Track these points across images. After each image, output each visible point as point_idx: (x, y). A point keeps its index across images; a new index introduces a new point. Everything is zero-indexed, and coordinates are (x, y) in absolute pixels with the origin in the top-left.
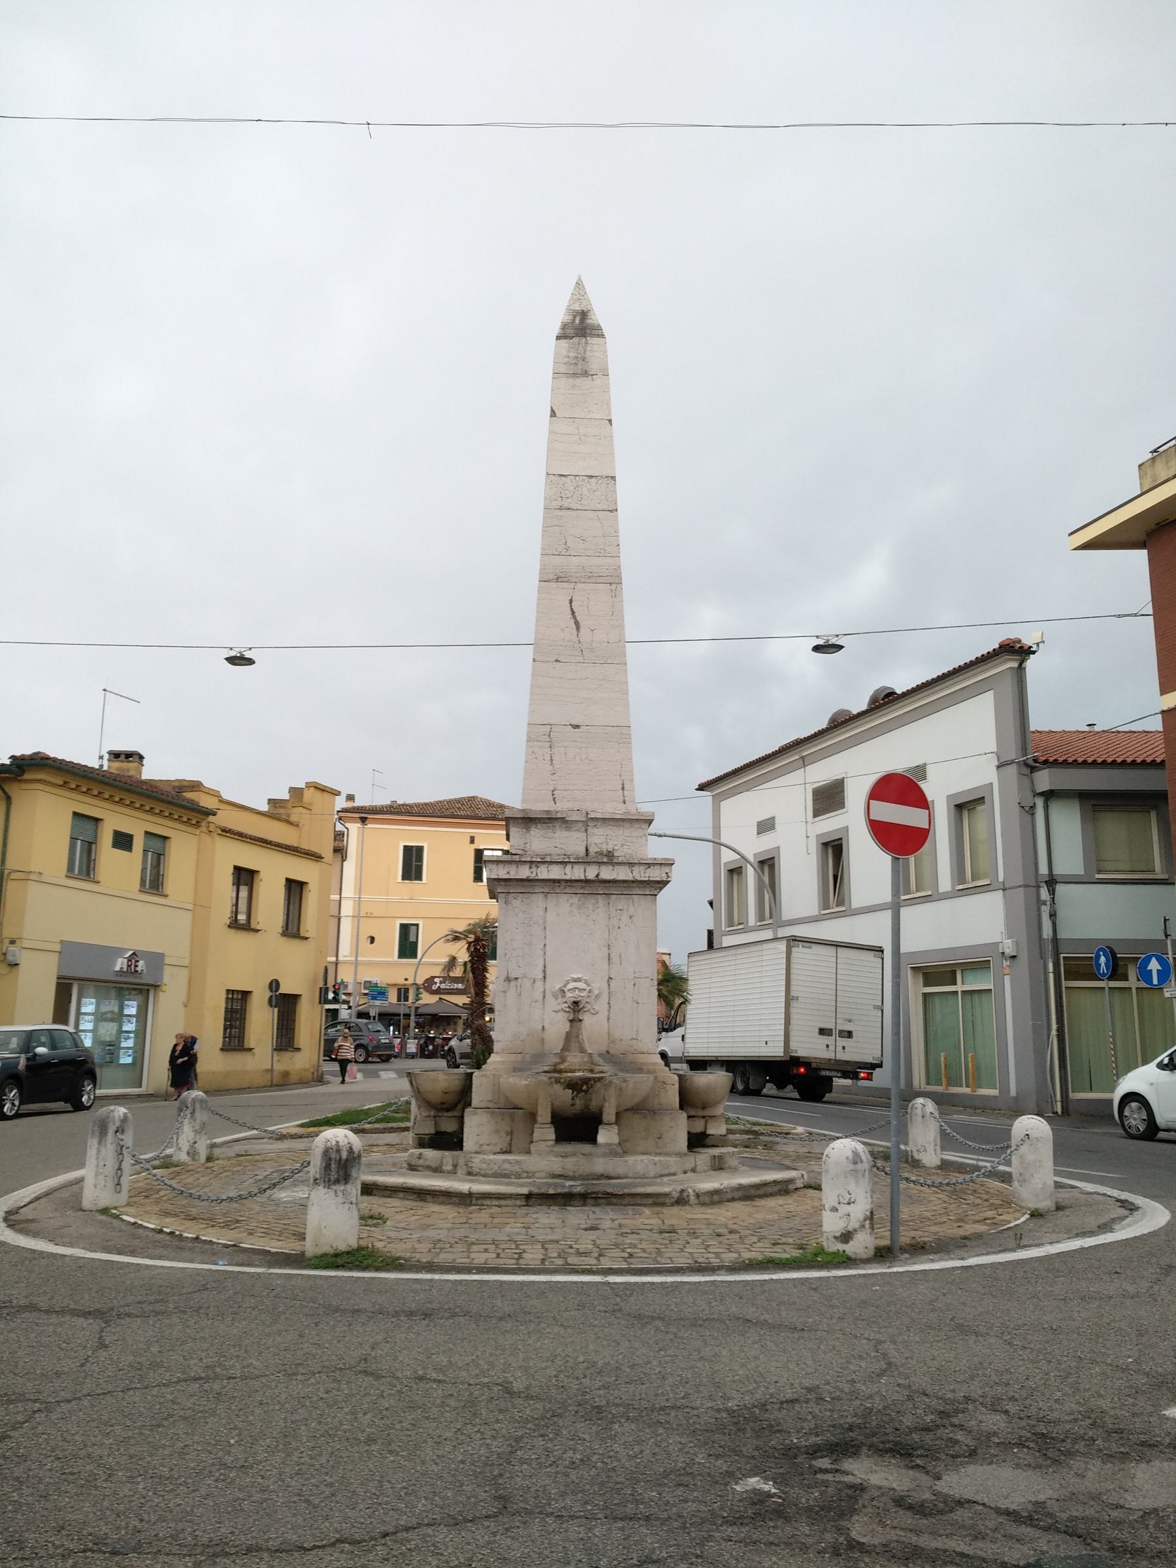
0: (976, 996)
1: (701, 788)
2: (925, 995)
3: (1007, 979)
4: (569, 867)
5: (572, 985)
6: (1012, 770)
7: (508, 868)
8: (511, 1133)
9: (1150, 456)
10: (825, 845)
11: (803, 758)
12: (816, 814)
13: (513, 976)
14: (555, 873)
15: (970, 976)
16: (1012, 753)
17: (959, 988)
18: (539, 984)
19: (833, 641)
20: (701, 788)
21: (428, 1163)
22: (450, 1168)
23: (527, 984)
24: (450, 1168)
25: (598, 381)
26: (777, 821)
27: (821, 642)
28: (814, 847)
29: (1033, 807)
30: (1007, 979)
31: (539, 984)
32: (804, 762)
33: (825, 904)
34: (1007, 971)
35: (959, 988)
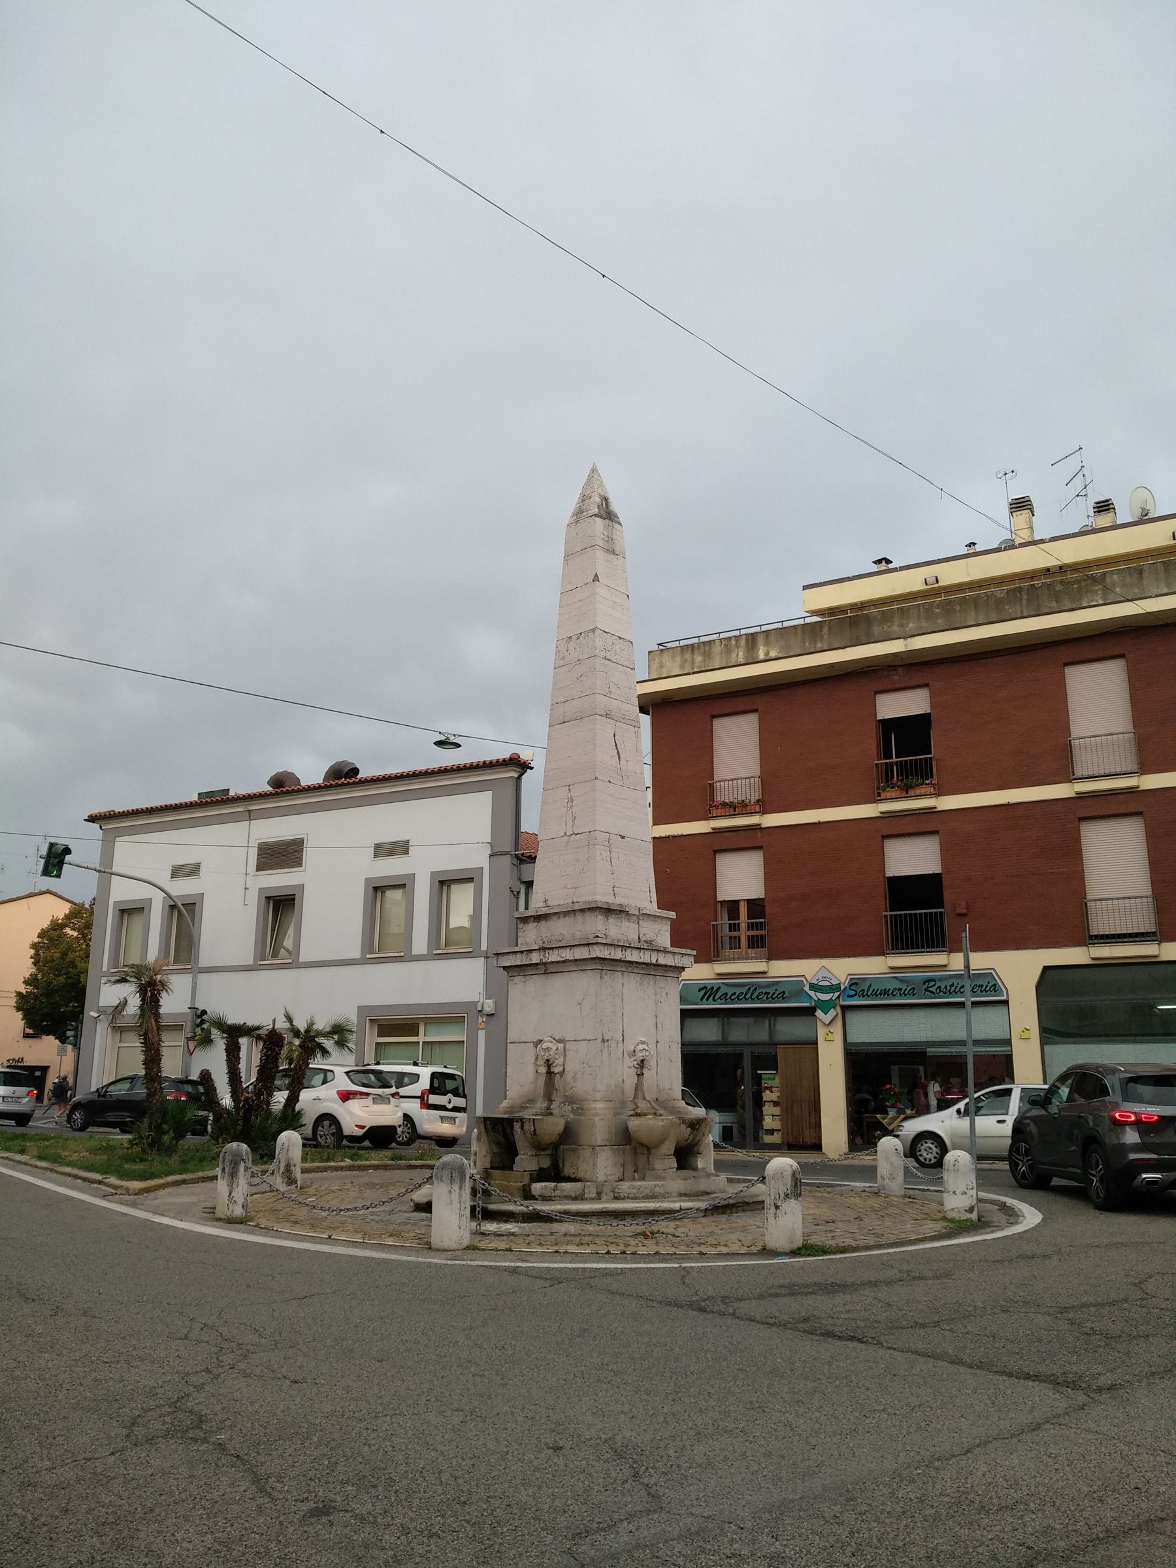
0: (437, 1048)
1: (92, 819)
2: (377, 1044)
3: (482, 1035)
4: (629, 951)
5: (641, 1047)
6: (507, 860)
7: (612, 950)
8: (623, 1165)
9: (656, 648)
10: (268, 898)
11: (249, 811)
12: (260, 868)
13: (606, 1038)
14: (567, 955)
15: (432, 1029)
16: (508, 846)
17: (421, 1038)
18: (620, 1045)
19: (452, 739)
20: (92, 819)
21: (565, 1193)
22: (594, 1195)
23: (614, 1044)
24: (594, 1195)
25: (620, 561)
26: (202, 869)
27: (443, 738)
28: (253, 900)
29: (518, 893)
30: (482, 1035)
31: (620, 1045)
32: (250, 816)
33: (260, 954)
34: (483, 1026)
35: (421, 1038)
